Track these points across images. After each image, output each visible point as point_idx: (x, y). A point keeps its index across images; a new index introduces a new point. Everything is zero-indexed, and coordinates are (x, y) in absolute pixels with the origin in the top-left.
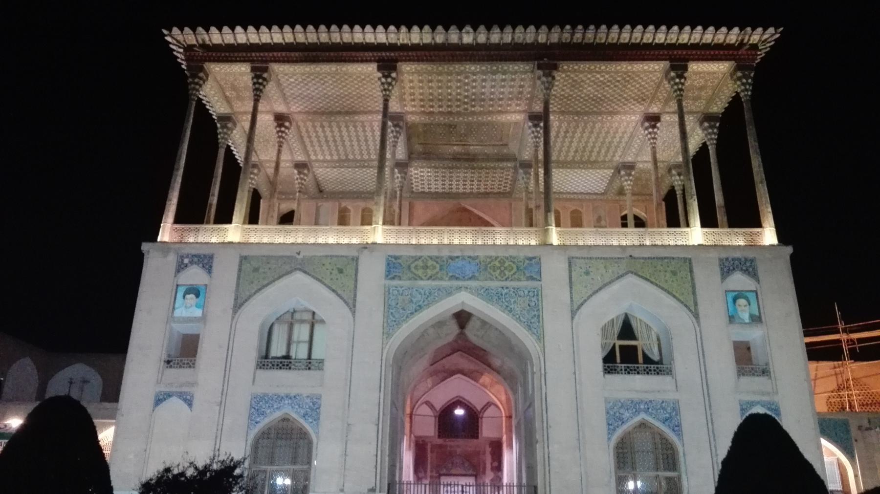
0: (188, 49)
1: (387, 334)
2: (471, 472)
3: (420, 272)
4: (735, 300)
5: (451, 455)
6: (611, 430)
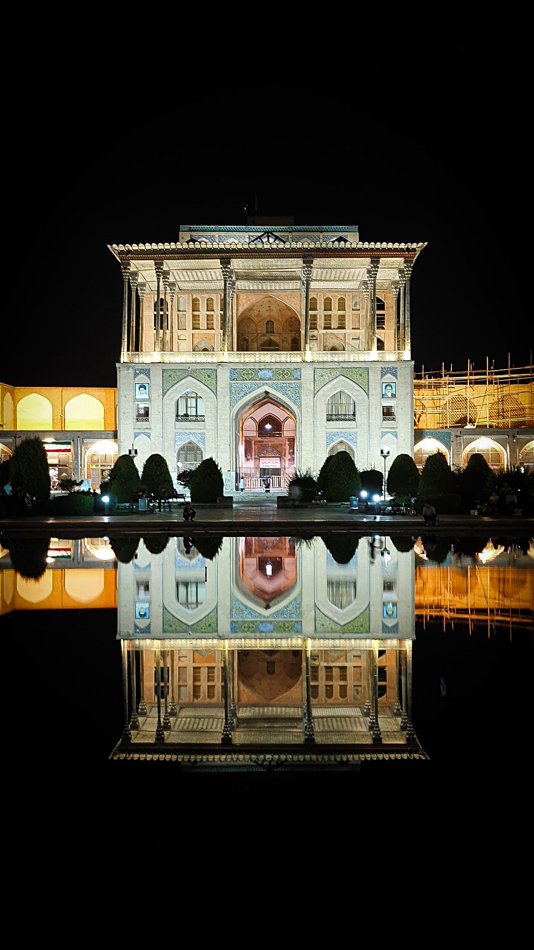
0: (121, 253)
1: (232, 406)
2: (277, 455)
3: (246, 377)
4: (386, 387)
5: (265, 447)
6: (327, 445)
